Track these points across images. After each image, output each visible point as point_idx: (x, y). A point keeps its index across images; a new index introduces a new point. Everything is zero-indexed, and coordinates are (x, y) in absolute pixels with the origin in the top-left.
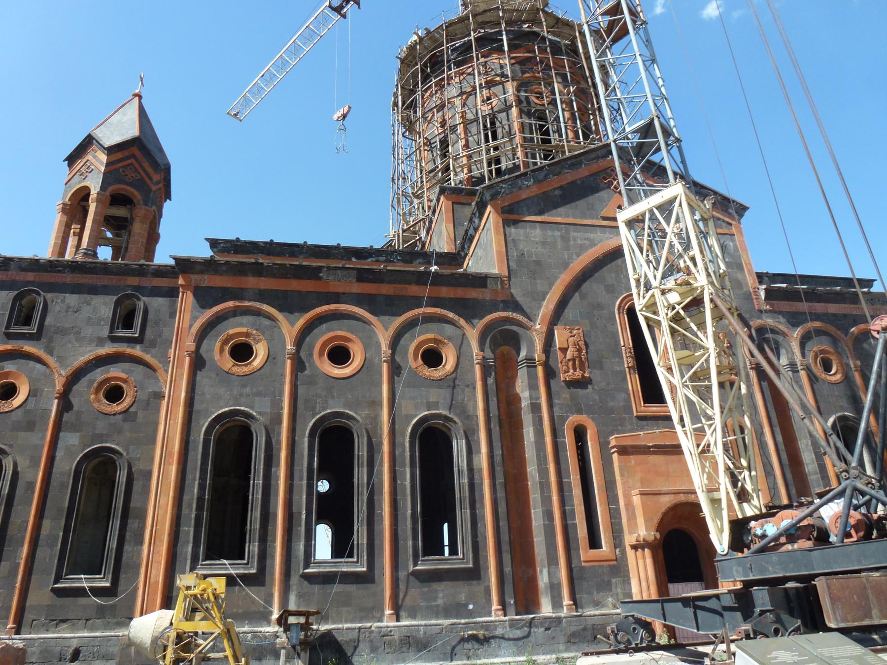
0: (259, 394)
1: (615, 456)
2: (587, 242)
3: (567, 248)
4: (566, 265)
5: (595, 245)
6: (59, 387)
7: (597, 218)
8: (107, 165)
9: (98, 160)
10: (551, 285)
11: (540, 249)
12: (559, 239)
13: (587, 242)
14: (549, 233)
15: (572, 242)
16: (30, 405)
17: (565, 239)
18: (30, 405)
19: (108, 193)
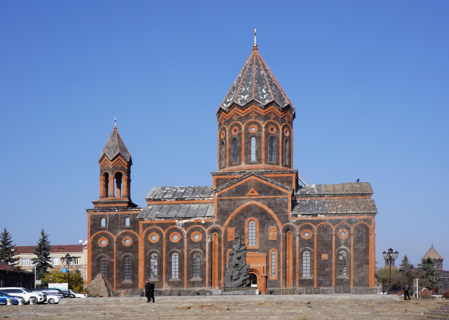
0: (158, 247)
10: (228, 217)
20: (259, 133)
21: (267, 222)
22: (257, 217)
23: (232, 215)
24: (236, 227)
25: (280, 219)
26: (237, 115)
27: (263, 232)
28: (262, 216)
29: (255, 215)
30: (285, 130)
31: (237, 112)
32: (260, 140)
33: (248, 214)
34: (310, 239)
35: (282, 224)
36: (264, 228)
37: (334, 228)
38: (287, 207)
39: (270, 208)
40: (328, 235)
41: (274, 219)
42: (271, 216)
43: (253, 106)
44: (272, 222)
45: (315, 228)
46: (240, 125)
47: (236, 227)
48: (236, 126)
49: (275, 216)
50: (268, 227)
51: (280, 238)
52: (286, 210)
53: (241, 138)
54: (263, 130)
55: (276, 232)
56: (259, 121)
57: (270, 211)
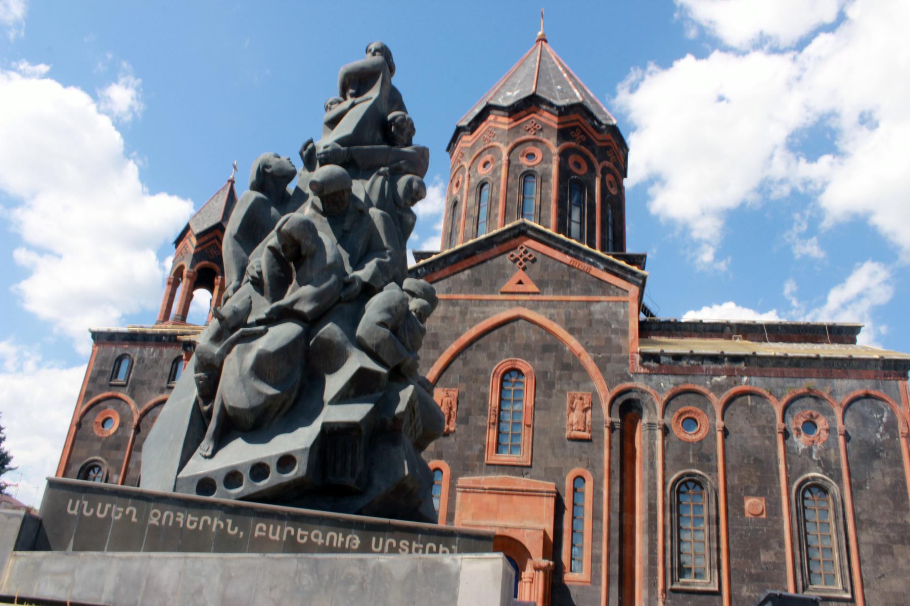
1: (459, 495)
2: (481, 316)
3: (463, 321)
4: (458, 335)
5: (488, 317)
6: (135, 422)
7: (497, 293)
8: (197, 247)
9: (191, 243)
10: (441, 353)
11: (439, 323)
12: (458, 315)
13: (481, 316)
14: (451, 308)
15: (468, 316)
16: (120, 433)
17: (463, 313)
18: (120, 433)
19: (195, 269)
20: (545, 166)
21: (560, 378)
22: (530, 359)
23: (453, 347)
24: (463, 387)
25: (602, 368)
26: (496, 129)
27: (547, 408)
28: (547, 355)
29: (526, 351)
30: (609, 177)
31: (492, 124)
32: (547, 181)
33: (501, 349)
34: (701, 441)
35: (610, 386)
36: (550, 397)
37: (778, 409)
38: (625, 333)
39: (571, 331)
40: (761, 429)
41: (582, 369)
42: (576, 357)
43: (533, 108)
44: (576, 376)
45: (717, 402)
46: (499, 148)
47: (463, 387)
48: (489, 153)
49: (587, 360)
50: (562, 392)
51: (602, 432)
52: (621, 341)
53: (499, 178)
54: (555, 159)
55: (589, 412)
56: (545, 140)
57: (572, 342)
